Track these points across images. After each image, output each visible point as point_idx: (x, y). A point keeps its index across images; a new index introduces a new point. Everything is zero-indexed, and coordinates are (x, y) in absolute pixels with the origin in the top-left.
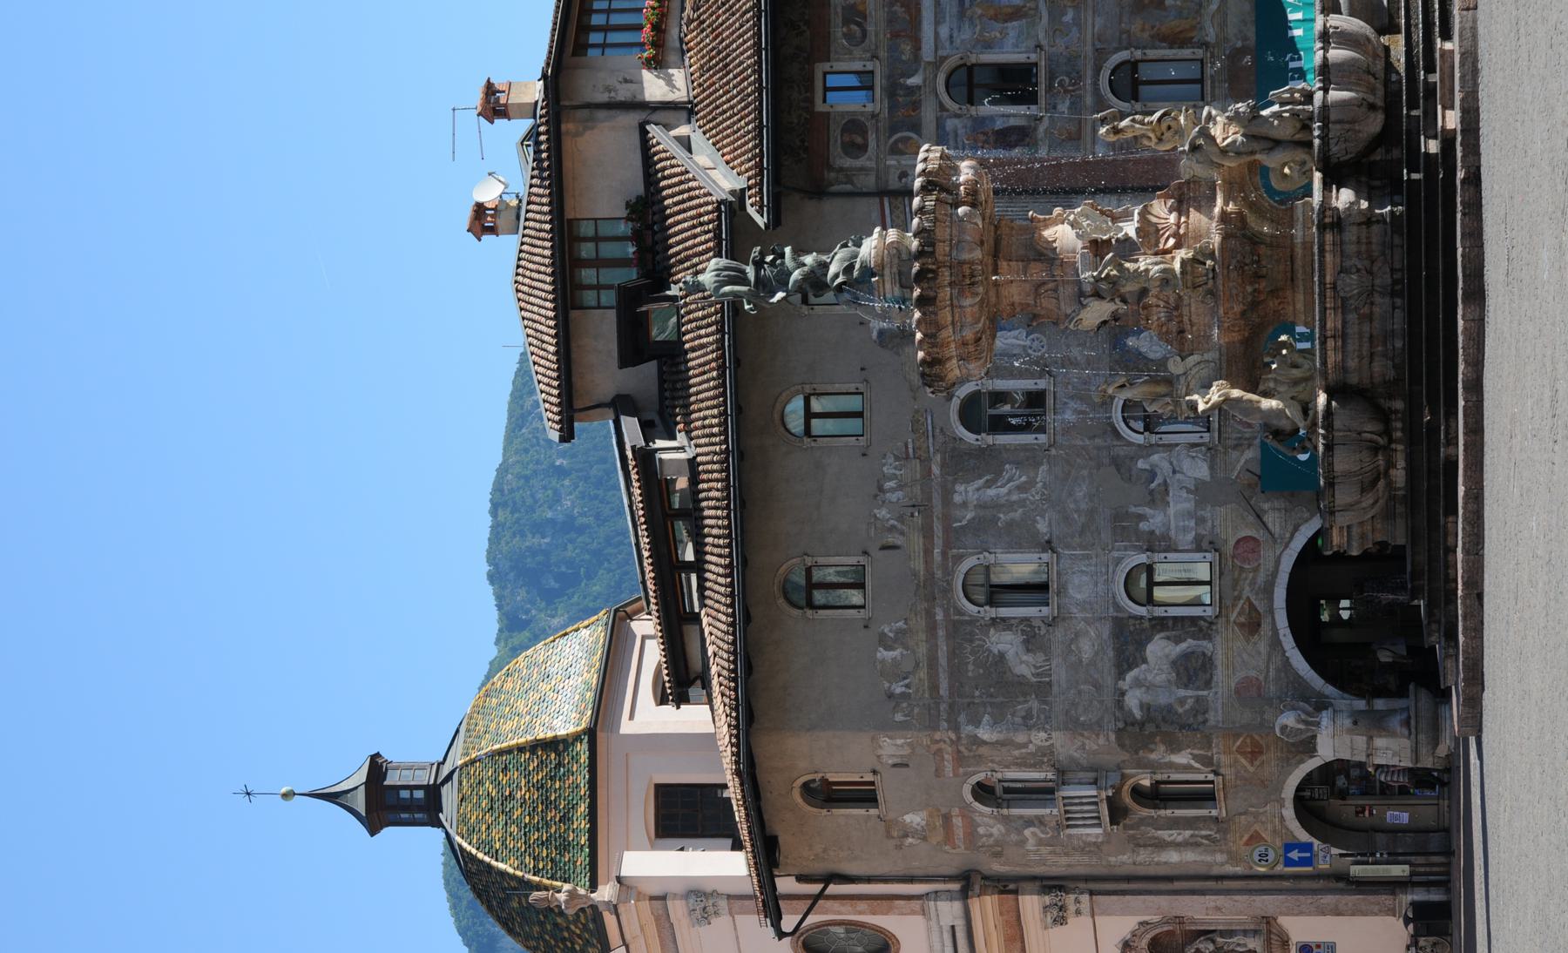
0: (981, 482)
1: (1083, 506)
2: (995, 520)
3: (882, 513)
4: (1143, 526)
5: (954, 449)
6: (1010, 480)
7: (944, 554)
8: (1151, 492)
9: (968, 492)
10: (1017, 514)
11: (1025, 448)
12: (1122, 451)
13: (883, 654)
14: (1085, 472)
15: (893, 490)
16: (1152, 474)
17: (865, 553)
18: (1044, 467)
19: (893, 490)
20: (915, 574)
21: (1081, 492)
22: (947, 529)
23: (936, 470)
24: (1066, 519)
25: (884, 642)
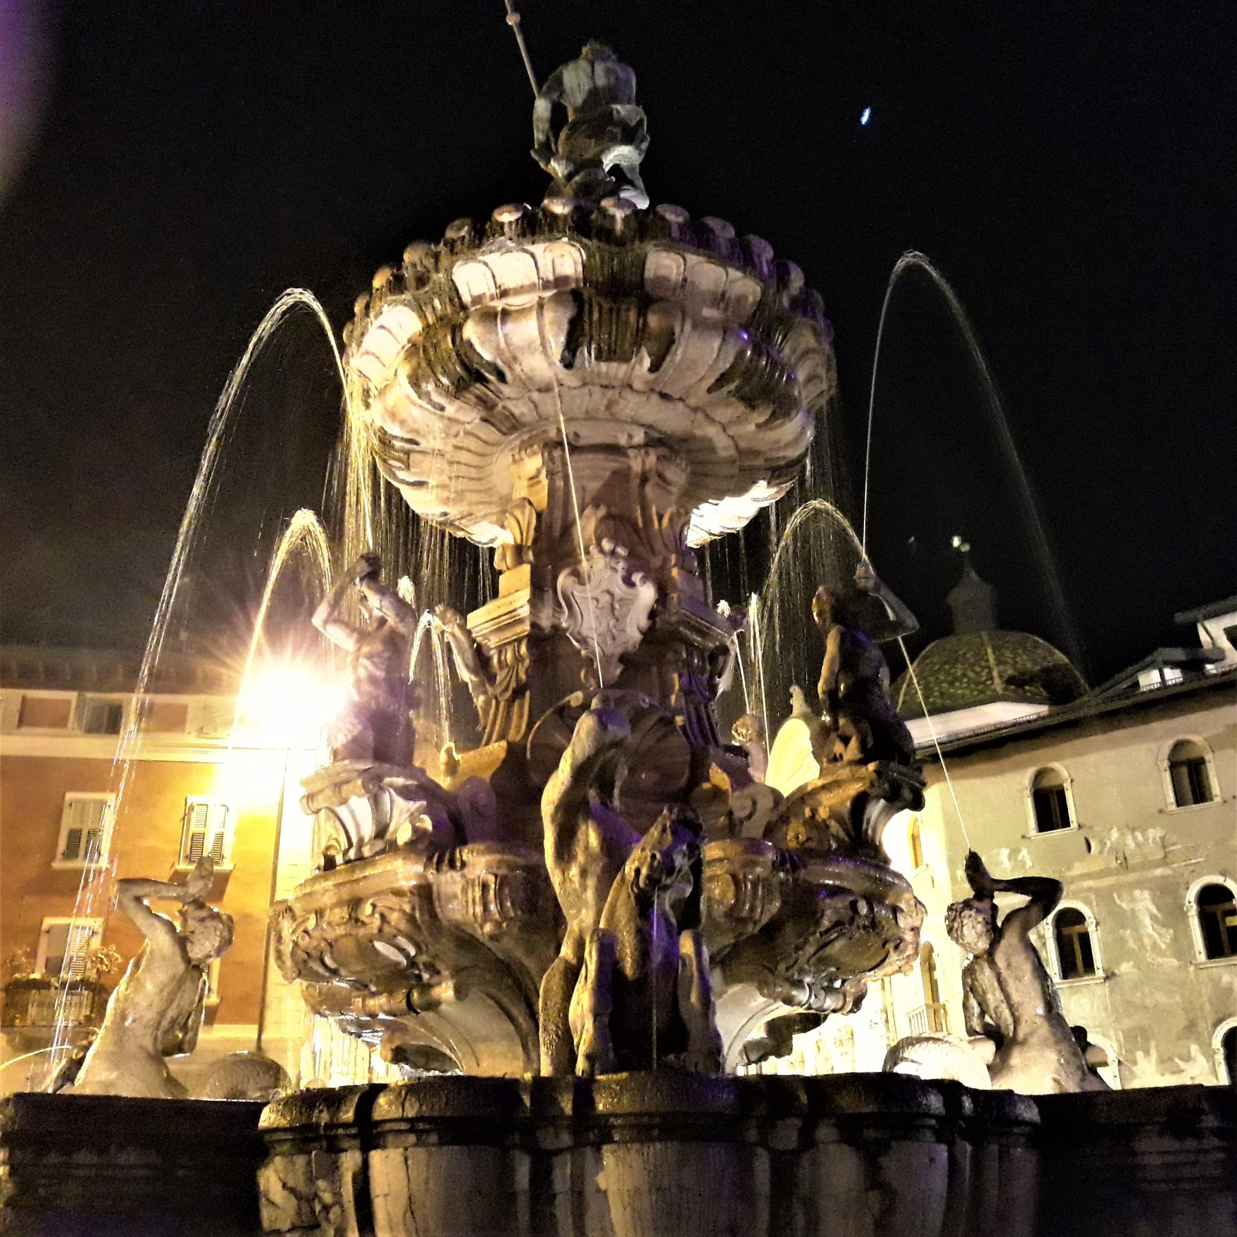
0: (1154, 910)
1: (1148, 1001)
2: (1124, 927)
3: (1115, 835)
4: (1140, 1055)
5: (1178, 884)
6: (1160, 935)
7: (1090, 889)
8: (1171, 1059)
9: (1144, 904)
10: (1131, 944)
11: (1191, 946)
12: (1203, 1026)
13: (1005, 852)
14: (1178, 999)
15: (1135, 838)
16: (1188, 1058)
17: (1080, 827)
18: (1174, 962)
19: (1135, 838)
20: (1069, 868)
21: (1161, 998)
22: (1111, 889)
23: (1158, 872)
24: (1136, 986)
25: (1014, 852)
